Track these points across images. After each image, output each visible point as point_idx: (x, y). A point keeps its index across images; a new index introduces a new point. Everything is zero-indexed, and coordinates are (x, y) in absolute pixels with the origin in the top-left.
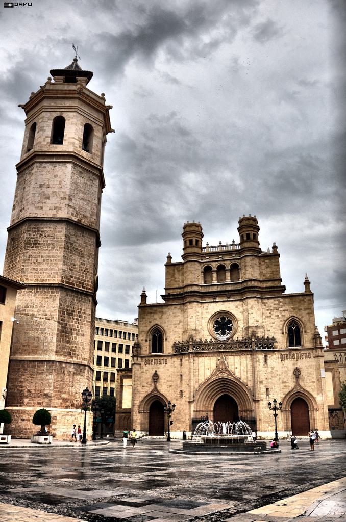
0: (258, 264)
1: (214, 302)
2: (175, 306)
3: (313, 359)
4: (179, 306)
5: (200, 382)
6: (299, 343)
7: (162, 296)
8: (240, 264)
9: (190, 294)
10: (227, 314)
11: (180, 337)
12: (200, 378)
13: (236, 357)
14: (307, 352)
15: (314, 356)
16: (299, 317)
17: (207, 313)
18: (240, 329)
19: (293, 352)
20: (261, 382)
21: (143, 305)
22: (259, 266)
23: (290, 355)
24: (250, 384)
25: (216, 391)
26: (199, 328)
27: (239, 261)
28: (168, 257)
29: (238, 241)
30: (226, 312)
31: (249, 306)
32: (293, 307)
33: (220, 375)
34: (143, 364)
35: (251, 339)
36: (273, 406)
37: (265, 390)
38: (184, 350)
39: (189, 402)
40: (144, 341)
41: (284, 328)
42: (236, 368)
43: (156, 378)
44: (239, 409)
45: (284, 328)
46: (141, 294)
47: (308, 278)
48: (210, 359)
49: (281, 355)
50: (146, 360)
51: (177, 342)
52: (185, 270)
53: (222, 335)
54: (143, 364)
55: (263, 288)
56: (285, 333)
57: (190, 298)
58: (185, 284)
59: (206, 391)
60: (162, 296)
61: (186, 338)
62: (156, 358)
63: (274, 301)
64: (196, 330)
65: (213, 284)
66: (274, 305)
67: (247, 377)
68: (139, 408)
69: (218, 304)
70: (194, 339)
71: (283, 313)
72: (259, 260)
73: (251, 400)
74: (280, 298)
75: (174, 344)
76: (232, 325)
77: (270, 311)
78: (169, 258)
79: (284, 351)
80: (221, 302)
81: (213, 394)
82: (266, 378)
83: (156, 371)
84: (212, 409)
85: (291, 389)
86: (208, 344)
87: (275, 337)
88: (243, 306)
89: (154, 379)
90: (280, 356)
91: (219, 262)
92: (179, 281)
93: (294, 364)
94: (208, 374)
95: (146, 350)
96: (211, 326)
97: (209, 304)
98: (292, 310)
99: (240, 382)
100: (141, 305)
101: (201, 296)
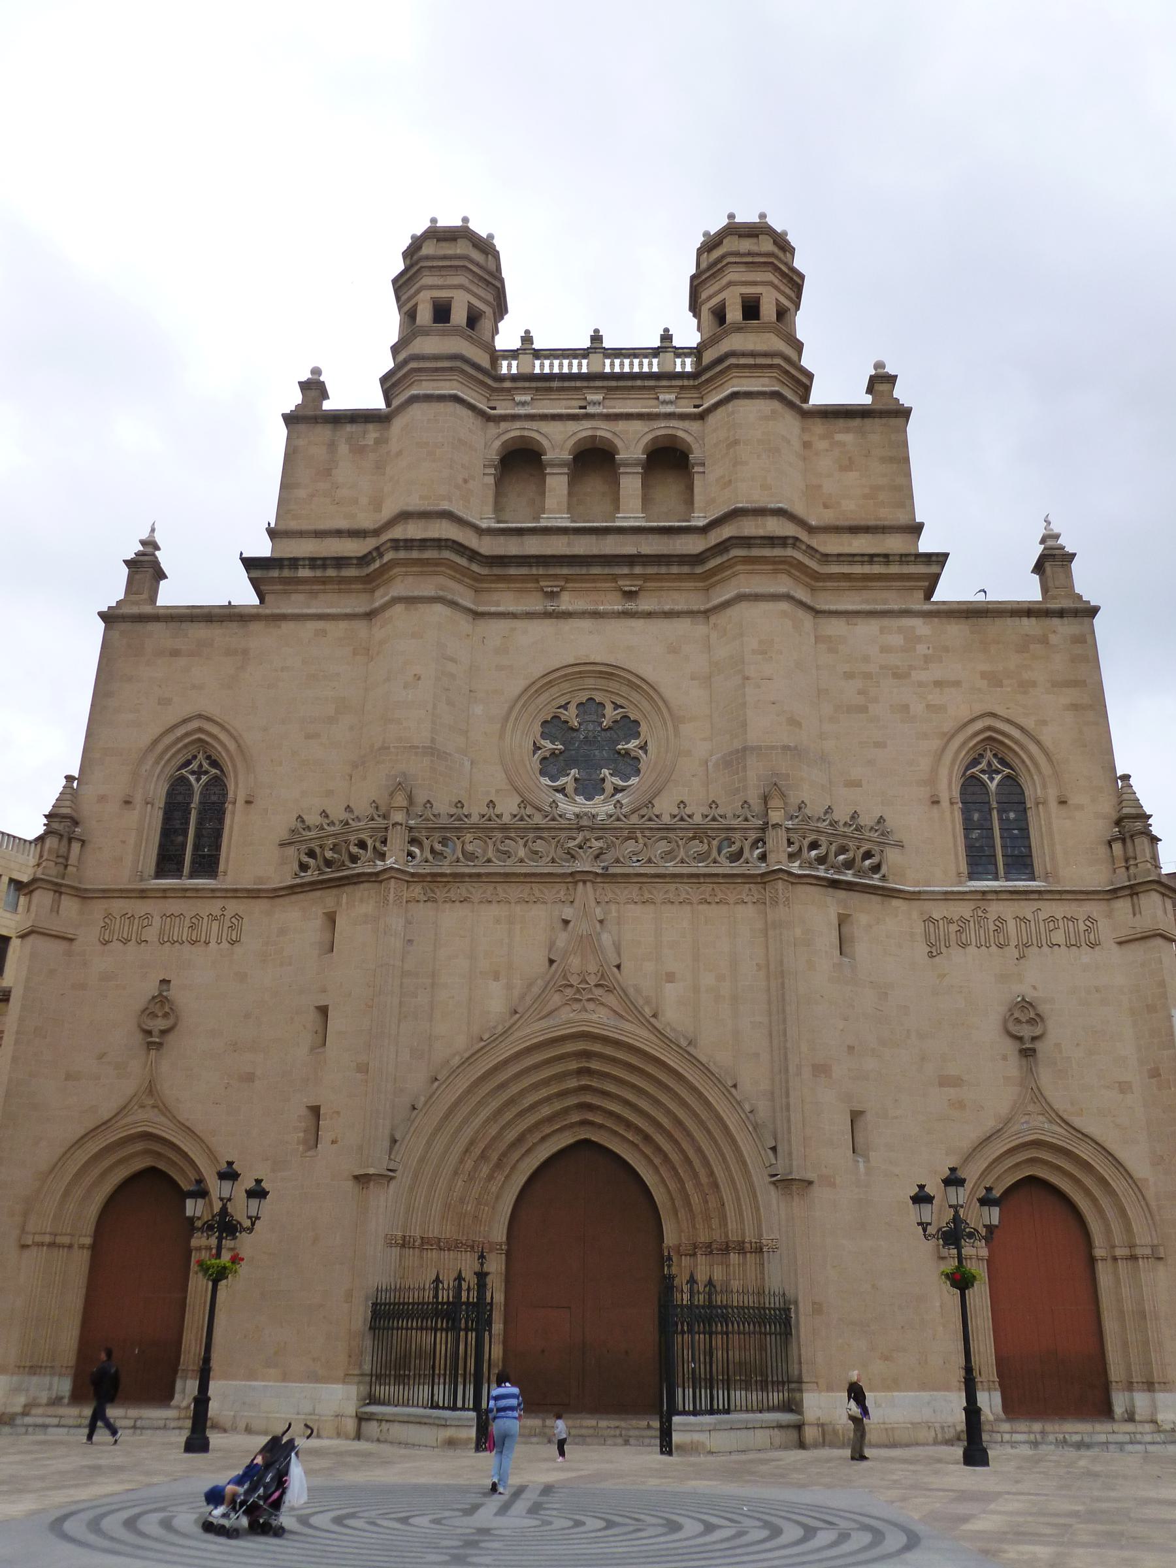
0: (796, 444)
2: (320, 624)
3: (1112, 954)
4: (343, 625)
6: (1021, 863)
7: (250, 563)
9: (415, 554)
10: (613, 686)
11: (329, 793)
15: (1124, 933)
16: (1021, 721)
19: (995, 909)
20: (821, 1070)
25: (531, 1119)
27: (694, 426)
28: (305, 386)
29: (688, 334)
30: (609, 673)
32: (986, 667)
33: (566, 1014)
38: (354, 859)
39: (357, 1178)
41: (944, 772)
42: (671, 977)
45: (944, 772)
46: (130, 556)
47: (1057, 537)
50: (108, 915)
51: (313, 819)
52: (394, 446)
53: (580, 799)
54: (88, 937)
55: (826, 558)
56: (945, 803)
58: (387, 512)
59: (473, 1113)
60: (250, 563)
62: (174, 906)
63: (882, 630)
65: (543, 524)
68: (26, 1215)
69: (567, 626)
70: (421, 797)
72: (803, 430)
76: (644, 747)
78: (314, 388)
79: (948, 896)
80: (583, 614)
81: (511, 1135)
82: (851, 1048)
84: (499, 1234)
85: (990, 1124)
86: (504, 828)
87: (890, 824)
90: (919, 929)
97: (518, 624)
98: (984, 684)
99: (694, 1061)
100: (126, 610)
101: (478, 578)
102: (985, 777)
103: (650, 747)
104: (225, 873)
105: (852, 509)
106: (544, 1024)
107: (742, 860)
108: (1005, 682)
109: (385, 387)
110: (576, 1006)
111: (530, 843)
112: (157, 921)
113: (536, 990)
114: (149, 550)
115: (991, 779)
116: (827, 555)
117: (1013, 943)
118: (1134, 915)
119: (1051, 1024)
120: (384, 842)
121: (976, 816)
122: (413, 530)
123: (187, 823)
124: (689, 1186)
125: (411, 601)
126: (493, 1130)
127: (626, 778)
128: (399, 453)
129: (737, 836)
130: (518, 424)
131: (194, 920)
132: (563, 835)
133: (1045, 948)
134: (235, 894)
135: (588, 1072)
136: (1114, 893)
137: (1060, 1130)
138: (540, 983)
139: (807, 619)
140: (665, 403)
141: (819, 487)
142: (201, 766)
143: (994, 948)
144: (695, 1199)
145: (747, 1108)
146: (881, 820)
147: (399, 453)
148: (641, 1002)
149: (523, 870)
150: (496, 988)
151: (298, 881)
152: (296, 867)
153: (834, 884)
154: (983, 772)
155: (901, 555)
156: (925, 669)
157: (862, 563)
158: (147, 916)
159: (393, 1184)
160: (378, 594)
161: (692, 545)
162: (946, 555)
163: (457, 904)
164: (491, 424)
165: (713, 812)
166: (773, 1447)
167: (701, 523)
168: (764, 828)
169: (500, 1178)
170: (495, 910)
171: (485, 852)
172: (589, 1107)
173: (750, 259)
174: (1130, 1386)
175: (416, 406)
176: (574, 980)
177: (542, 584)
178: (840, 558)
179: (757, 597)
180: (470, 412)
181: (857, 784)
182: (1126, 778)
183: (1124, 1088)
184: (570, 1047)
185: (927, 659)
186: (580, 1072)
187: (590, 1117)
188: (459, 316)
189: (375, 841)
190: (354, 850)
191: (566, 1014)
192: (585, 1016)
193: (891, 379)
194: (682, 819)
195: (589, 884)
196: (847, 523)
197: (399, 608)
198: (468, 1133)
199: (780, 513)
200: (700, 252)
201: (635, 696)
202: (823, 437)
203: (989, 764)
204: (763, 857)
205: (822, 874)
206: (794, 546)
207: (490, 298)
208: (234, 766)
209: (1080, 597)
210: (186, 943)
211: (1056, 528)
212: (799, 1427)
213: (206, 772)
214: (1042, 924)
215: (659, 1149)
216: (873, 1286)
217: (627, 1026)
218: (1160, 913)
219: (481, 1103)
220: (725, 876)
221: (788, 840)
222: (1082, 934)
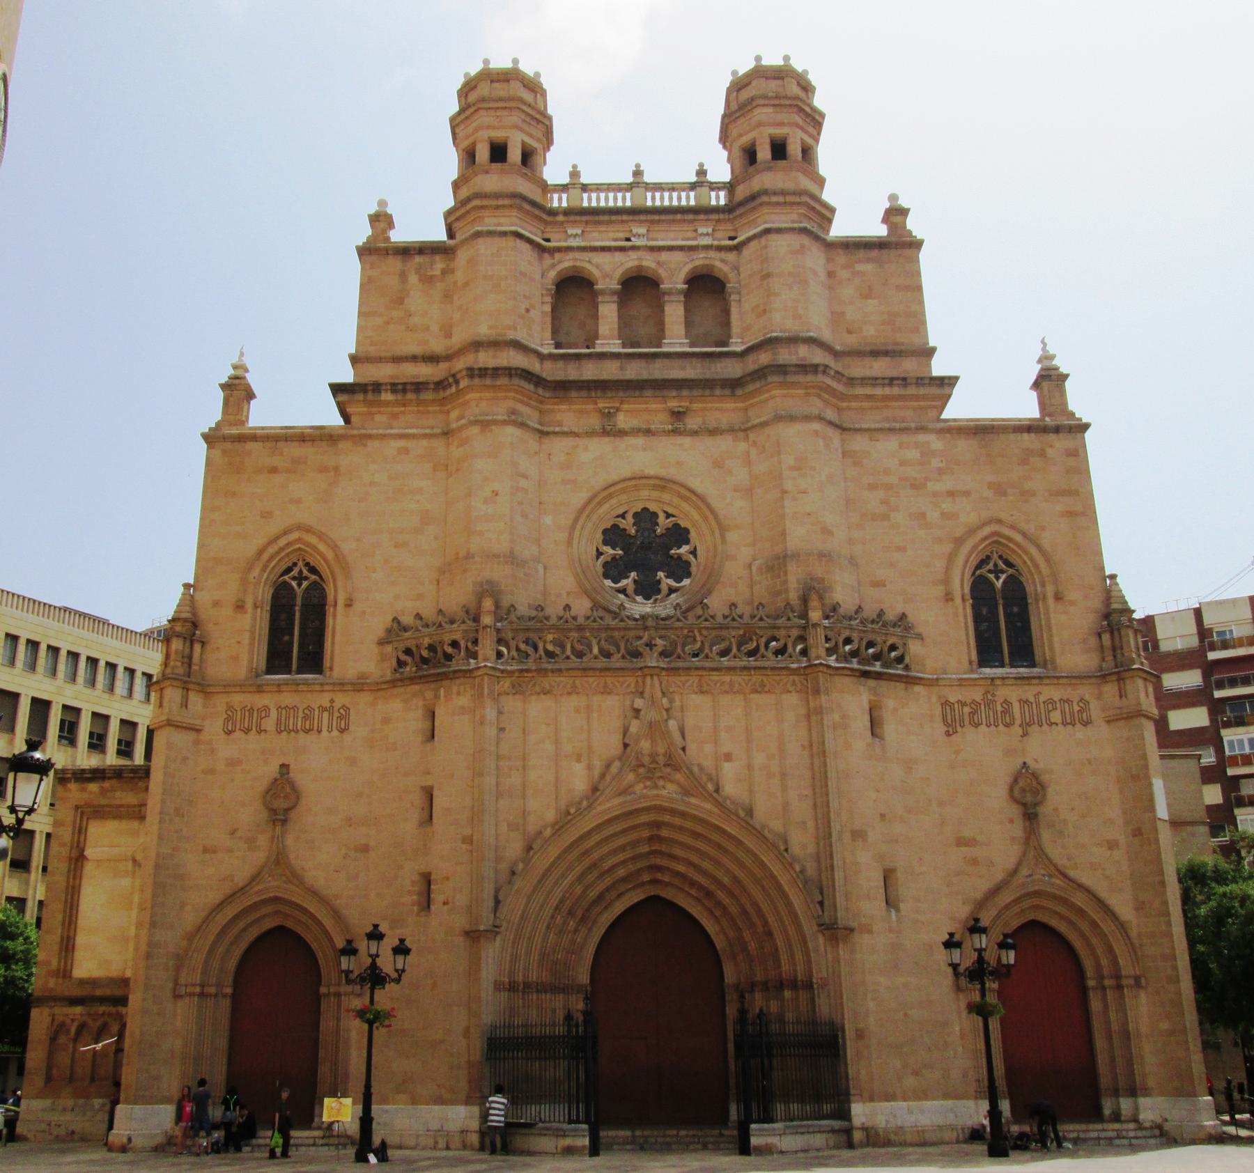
0: (822, 275)
1: (605, 433)
2: (402, 443)
3: (1101, 731)
4: (424, 443)
5: (533, 825)
6: (1023, 652)
7: (337, 389)
8: (736, 268)
10: (666, 497)
11: (420, 597)
12: (532, 804)
13: (725, 700)
14: (1074, 694)
17: (564, 482)
18: (733, 570)
19: (1002, 693)
21: (234, 431)
22: (830, 288)
23: (989, 704)
24: (802, 842)
26: (527, 551)
27: (731, 257)
29: (721, 171)
30: (663, 484)
31: (789, 460)
34: (213, 728)
35: (804, 615)
36: (966, 959)
37: (877, 877)
38: (449, 657)
40: (227, 611)
42: (728, 757)
43: (280, 804)
44: (730, 974)
46: (224, 380)
47: (1052, 357)
48: (589, 709)
49: (946, 704)
50: (230, 707)
51: (407, 620)
52: (460, 276)
53: (639, 599)
54: (213, 728)
55: (851, 381)
57: (483, 404)
58: (460, 337)
59: (563, 876)
60: (337, 389)
61: (457, 596)
62: (288, 699)
63: (901, 446)
64: (511, 558)
66: (902, 463)
67: (786, 805)
70: (505, 603)
71: (947, 506)
72: (829, 260)
73: (809, 928)
74: (932, 438)
75: (389, 631)
76: (694, 552)
77: (881, 494)
78: (381, 220)
79: (961, 683)
81: (593, 894)
82: (883, 816)
83: (284, 767)
84: (583, 977)
85: (999, 876)
86: (580, 628)
87: (911, 618)
88: (749, 463)
89: (273, 811)
90: (938, 711)
91: (633, 255)
92: (427, 329)
93: (1009, 752)
94: (578, 780)
95: (236, 658)
96: (589, 541)
97: (582, 442)
98: (989, 494)
102: (992, 576)
103: (699, 552)
104: (331, 669)
105: (871, 333)
106: (621, 799)
107: (786, 655)
108: (1009, 491)
109: (449, 221)
110: (648, 783)
111: (603, 642)
112: (274, 713)
113: (614, 769)
114: (239, 372)
115: (998, 578)
116: (852, 379)
117: (1018, 722)
118: (1121, 697)
119: (1051, 792)
120: (475, 642)
121: (984, 611)
122: (486, 359)
123: (293, 624)
124: (747, 935)
125: (485, 425)
126: (579, 889)
127: (679, 580)
128: (466, 284)
129: (783, 632)
130: (571, 255)
131: (306, 711)
132: (632, 634)
133: (1045, 727)
134: (341, 686)
135: (660, 839)
136: (1104, 677)
137: (1058, 882)
138: (617, 764)
139: (835, 436)
140: (702, 234)
141: (843, 313)
142: (301, 572)
143: (1001, 727)
144: (752, 945)
145: (798, 868)
146: (903, 616)
147: (466, 284)
148: (705, 779)
149: (599, 666)
150: (579, 768)
151: (398, 675)
152: (394, 663)
153: (866, 674)
154: (990, 571)
155: (918, 378)
156: (938, 481)
157: (883, 385)
158: (266, 709)
159: (499, 938)
160: (454, 415)
161: (732, 369)
162: (956, 379)
163: (542, 696)
164: (546, 255)
165: (761, 613)
166: (828, 1147)
167: (739, 349)
168: (804, 628)
169: (584, 931)
170: (574, 701)
171: (564, 651)
172: (659, 868)
173: (776, 102)
174: (1116, 1093)
175: (480, 240)
176: (646, 760)
177: (601, 405)
178: (864, 381)
179: (792, 418)
180: (528, 246)
181: (879, 584)
182: (1113, 577)
183: (1112, 845)
184: (644, 818)
185: (940, 471)
186: (651, 839)
187: (659, 876)
188: (515, 154)
189: (467, 641)
190: (449, 650)
191: (639, 788)
192: (655, 792)
193: (904, 212)
194: (734, 619)
195: (655, 678)
196: (868, 348)
197: (475, 430)
198: (557, 895)
199: (811, 341)
200: (729, 91)
201: (685, 506)
202: (846, 267)
203: (996, 565)
204: (804, 652)
205: (855, 666)
206: (824, 372)
207: (540, 135)
208: (332, 573)
209: (1073, 414)
210: (301, 733)
211: (1051, 350)
212: (848, 1131)
213: (306, 578)
214: (1042, 705)
215: (719, 904)
216: (905, 1015)
217: (693, 800)
218: (1142, 695)
219: (570, 868)
220: (773, 669)
221: (826, 637)
222: (1076, 715)
